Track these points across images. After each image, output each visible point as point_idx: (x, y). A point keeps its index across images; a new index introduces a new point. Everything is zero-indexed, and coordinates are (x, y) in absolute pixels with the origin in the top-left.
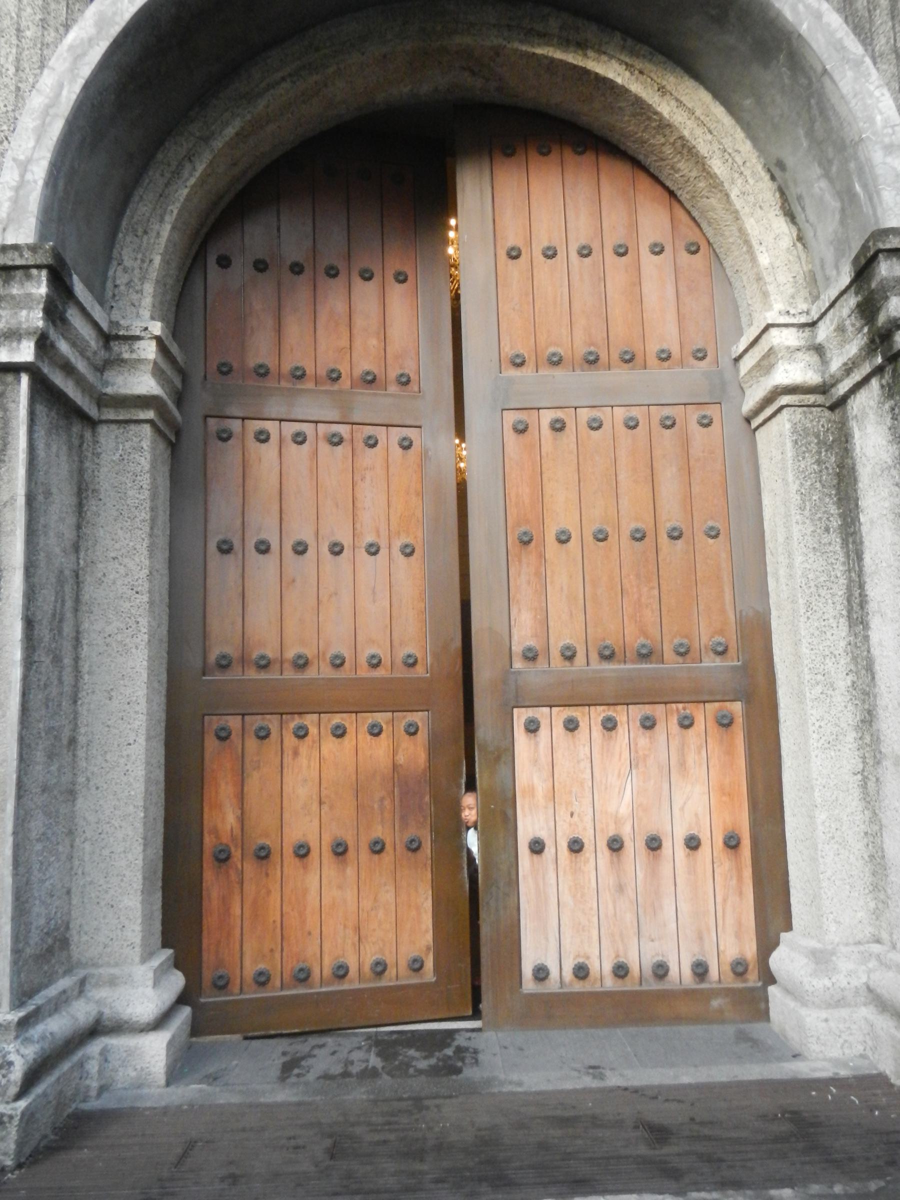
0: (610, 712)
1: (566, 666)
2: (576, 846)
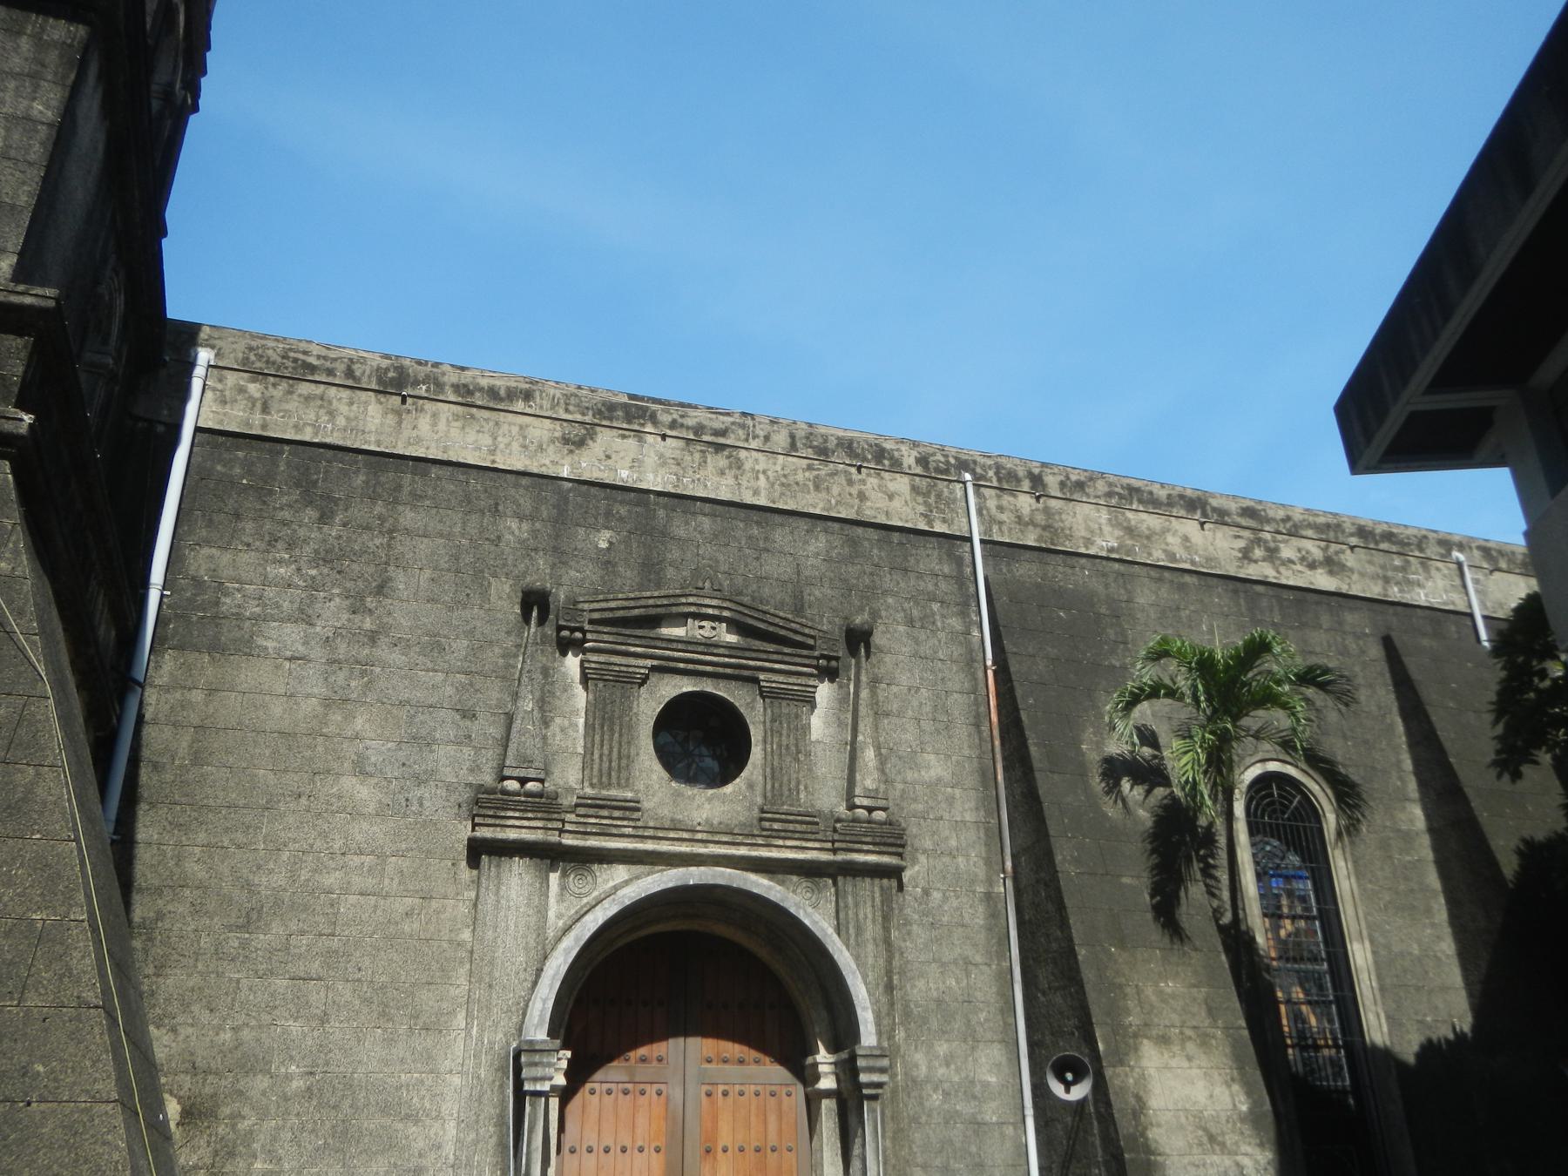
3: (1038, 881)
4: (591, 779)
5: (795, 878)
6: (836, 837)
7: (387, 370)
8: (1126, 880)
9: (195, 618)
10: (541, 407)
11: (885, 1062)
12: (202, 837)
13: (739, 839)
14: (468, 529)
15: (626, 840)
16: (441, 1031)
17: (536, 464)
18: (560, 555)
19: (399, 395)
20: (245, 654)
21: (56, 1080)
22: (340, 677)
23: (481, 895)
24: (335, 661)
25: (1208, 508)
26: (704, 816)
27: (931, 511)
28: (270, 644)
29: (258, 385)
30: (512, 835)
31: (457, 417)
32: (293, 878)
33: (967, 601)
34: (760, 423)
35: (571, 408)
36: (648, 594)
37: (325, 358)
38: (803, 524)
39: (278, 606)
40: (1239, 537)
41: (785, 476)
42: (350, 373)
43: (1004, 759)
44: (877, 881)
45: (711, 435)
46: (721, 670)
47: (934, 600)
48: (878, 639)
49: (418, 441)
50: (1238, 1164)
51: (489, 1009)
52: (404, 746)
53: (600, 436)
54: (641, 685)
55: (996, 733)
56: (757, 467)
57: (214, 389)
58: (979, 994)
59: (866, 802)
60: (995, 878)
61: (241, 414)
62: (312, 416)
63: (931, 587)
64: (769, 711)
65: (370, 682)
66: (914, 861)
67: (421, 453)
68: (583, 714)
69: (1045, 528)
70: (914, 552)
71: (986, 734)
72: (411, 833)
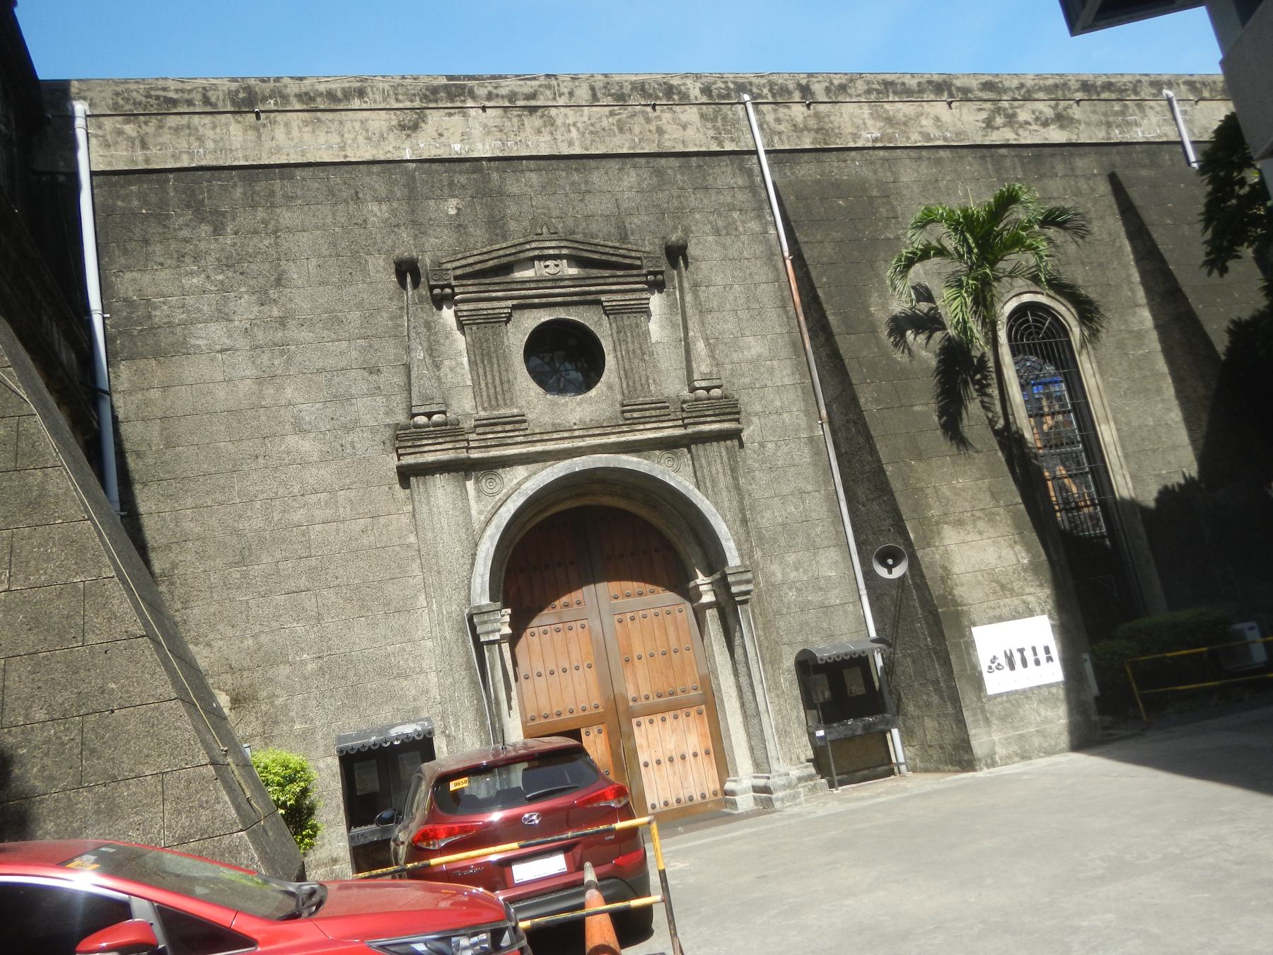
0: (663, 715)
1: (647, 702)
2: (658, 762)
3: (848, 421)
4: (482, 404)
5: (657, 452)
6: (685, 415)
7: (237, 92)
8: (916, 408)
9: (135, 333)
10: (375, 101)
11: (749, 576)
12: (190, 501)
13: (609, 430)
14: (338, 218)
15: (520, 446)
16: (409, 611)
17: (381, 152)
18: (419, 227)
19: (253, 112)
20: (184, 354)
21: (127, 692)
22: (265, 358)
23: (417, 507)
24: (257, 347)
25: (953, 88)
26: (578, 417)
27: (720, 134)
28: (200, 342)
29: (132, 126)
30: (430, 458)
31: (306, 123)
32: (268, 520)
33: (761, 206)
34: (563, 81)
35: (400, 97)
36: (498, 246)
37: (182, 91)
38: (614, 164)
39: (200, 311)
40: (982, 109)
41: (592, 125)
42: (206, 100)
43: (809, 330)
44: (722, 443)
45: (524, 99)
46: (569, 299)
47: (734, 209)
48: (692, 250)
49: (279, 149)
50: (1024, 602)
51: (442, 590)
52: (329, 404)
53: (430, 117)
54: (507, 322)
55: (800, 310)
56: (567, 122)
57: (96, 136)
58: (814, 515)
59: (704, 384)
60: (814, 425)
61: (125, 153)
62: (185, 144)
63: (729, 199)
64: (614, 325)
65: (289, 358)
66: (749, 423)
67: (283, 160)
68: (465, 354)
69: (817, 131)
70: (711, 171)
71: (792, 313)
72: (351, 470)
